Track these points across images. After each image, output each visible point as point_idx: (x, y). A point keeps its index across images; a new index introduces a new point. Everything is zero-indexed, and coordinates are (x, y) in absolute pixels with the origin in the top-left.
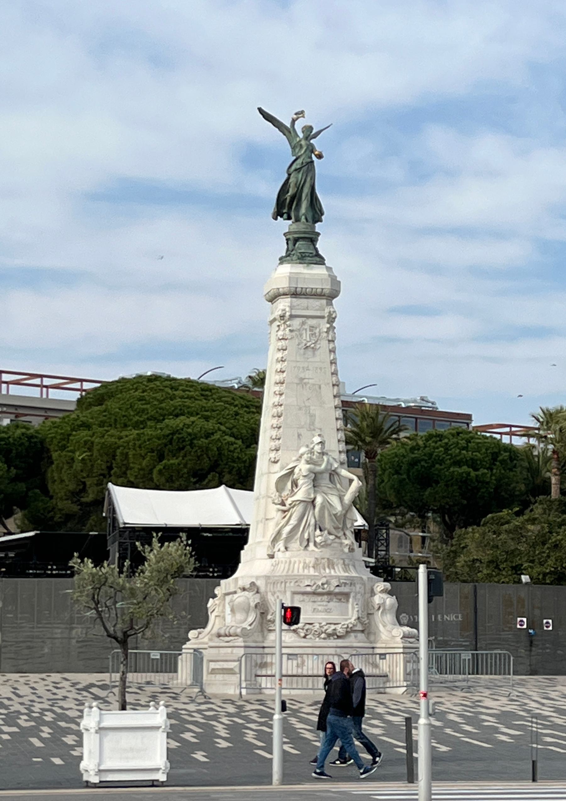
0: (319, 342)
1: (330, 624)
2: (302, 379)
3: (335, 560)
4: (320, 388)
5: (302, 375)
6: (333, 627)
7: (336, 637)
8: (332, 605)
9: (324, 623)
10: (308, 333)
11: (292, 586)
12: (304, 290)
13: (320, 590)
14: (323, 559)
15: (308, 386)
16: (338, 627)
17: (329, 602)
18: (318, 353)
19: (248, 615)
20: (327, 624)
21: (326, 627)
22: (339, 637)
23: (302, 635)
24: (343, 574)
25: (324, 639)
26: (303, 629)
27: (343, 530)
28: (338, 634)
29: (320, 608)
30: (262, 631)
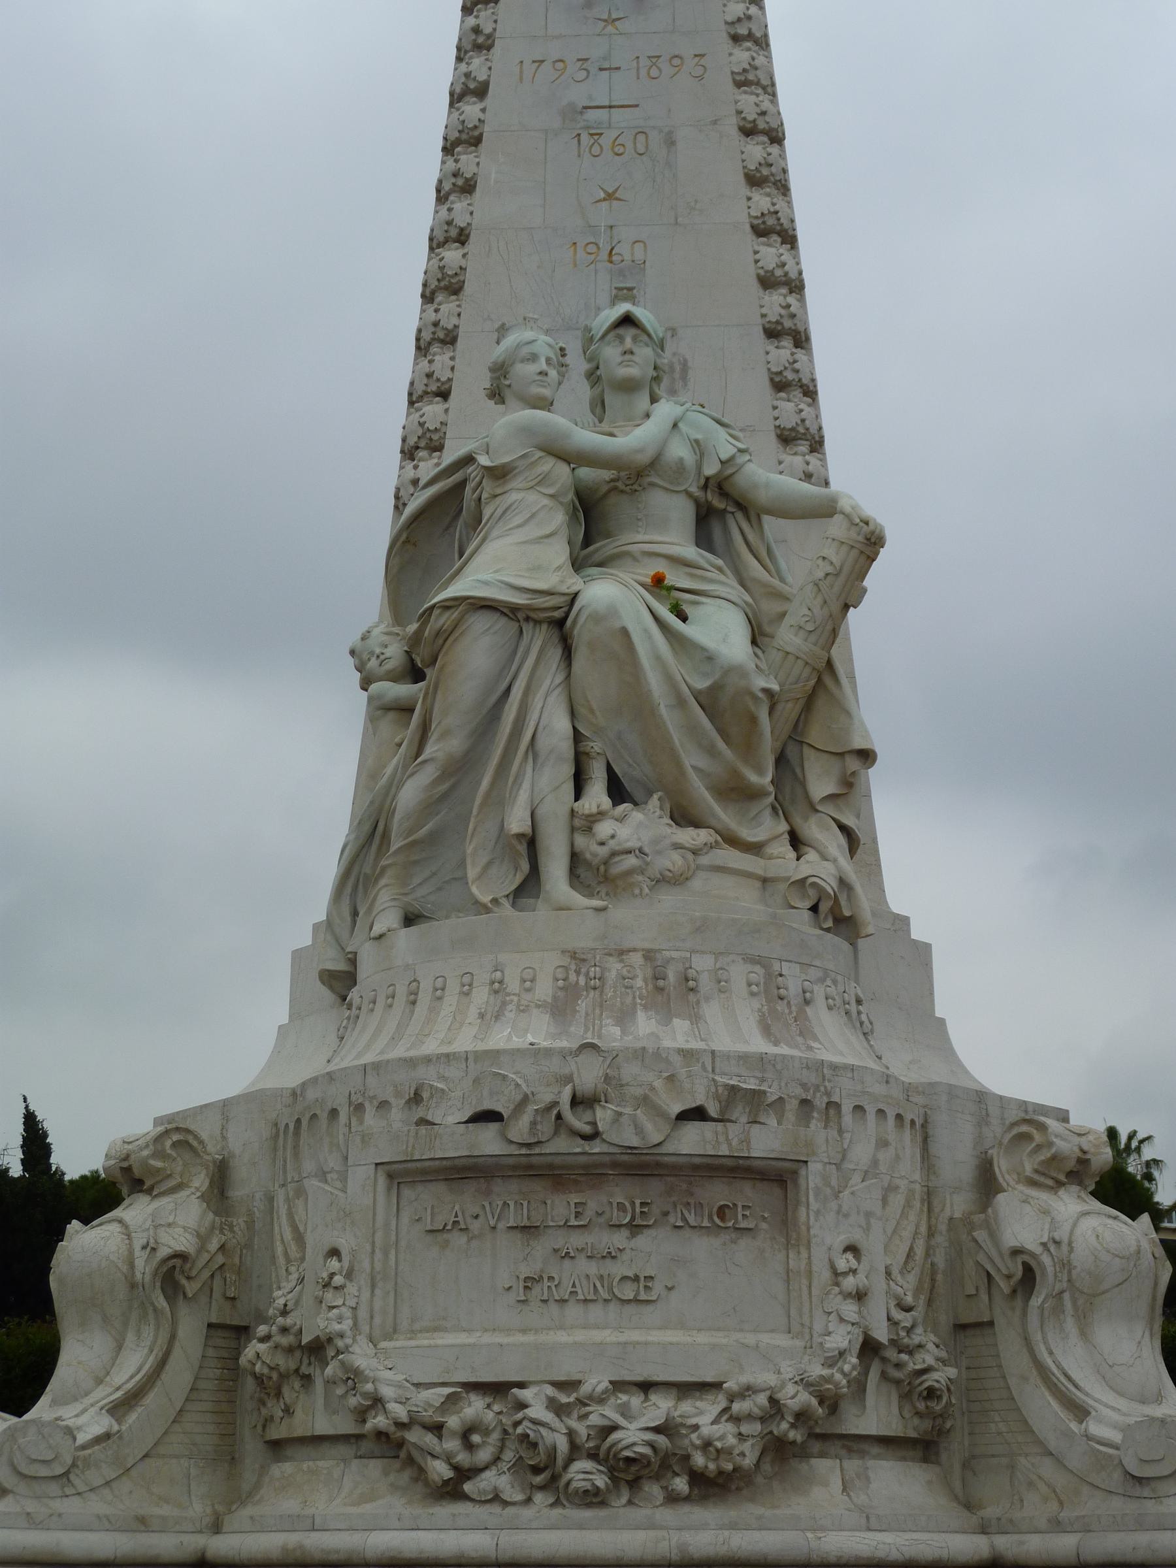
1: (646, 1387)
2: (574, 112)
3: (702, 963)
5: (577, 95)
6: (661, 1407)
7: (681, 1484)
8: (651, 1251)
9: (596, 1382)
11: (387, 1135)
13: (563, 1145)
14: (621, 953)
15: (606, 141)
16: (703, 1414)
17: (635, 1228)
19: (119, 1347)
20: (618, 1386)
21: (599, 1415)
22: (713, 1485)
23: (440, 1470)
24: (759, 1045)
25: (592, 1498)
26: (437, 1429)
27: (780, 809)
28: (699, 1460)
30: (226, 1456)
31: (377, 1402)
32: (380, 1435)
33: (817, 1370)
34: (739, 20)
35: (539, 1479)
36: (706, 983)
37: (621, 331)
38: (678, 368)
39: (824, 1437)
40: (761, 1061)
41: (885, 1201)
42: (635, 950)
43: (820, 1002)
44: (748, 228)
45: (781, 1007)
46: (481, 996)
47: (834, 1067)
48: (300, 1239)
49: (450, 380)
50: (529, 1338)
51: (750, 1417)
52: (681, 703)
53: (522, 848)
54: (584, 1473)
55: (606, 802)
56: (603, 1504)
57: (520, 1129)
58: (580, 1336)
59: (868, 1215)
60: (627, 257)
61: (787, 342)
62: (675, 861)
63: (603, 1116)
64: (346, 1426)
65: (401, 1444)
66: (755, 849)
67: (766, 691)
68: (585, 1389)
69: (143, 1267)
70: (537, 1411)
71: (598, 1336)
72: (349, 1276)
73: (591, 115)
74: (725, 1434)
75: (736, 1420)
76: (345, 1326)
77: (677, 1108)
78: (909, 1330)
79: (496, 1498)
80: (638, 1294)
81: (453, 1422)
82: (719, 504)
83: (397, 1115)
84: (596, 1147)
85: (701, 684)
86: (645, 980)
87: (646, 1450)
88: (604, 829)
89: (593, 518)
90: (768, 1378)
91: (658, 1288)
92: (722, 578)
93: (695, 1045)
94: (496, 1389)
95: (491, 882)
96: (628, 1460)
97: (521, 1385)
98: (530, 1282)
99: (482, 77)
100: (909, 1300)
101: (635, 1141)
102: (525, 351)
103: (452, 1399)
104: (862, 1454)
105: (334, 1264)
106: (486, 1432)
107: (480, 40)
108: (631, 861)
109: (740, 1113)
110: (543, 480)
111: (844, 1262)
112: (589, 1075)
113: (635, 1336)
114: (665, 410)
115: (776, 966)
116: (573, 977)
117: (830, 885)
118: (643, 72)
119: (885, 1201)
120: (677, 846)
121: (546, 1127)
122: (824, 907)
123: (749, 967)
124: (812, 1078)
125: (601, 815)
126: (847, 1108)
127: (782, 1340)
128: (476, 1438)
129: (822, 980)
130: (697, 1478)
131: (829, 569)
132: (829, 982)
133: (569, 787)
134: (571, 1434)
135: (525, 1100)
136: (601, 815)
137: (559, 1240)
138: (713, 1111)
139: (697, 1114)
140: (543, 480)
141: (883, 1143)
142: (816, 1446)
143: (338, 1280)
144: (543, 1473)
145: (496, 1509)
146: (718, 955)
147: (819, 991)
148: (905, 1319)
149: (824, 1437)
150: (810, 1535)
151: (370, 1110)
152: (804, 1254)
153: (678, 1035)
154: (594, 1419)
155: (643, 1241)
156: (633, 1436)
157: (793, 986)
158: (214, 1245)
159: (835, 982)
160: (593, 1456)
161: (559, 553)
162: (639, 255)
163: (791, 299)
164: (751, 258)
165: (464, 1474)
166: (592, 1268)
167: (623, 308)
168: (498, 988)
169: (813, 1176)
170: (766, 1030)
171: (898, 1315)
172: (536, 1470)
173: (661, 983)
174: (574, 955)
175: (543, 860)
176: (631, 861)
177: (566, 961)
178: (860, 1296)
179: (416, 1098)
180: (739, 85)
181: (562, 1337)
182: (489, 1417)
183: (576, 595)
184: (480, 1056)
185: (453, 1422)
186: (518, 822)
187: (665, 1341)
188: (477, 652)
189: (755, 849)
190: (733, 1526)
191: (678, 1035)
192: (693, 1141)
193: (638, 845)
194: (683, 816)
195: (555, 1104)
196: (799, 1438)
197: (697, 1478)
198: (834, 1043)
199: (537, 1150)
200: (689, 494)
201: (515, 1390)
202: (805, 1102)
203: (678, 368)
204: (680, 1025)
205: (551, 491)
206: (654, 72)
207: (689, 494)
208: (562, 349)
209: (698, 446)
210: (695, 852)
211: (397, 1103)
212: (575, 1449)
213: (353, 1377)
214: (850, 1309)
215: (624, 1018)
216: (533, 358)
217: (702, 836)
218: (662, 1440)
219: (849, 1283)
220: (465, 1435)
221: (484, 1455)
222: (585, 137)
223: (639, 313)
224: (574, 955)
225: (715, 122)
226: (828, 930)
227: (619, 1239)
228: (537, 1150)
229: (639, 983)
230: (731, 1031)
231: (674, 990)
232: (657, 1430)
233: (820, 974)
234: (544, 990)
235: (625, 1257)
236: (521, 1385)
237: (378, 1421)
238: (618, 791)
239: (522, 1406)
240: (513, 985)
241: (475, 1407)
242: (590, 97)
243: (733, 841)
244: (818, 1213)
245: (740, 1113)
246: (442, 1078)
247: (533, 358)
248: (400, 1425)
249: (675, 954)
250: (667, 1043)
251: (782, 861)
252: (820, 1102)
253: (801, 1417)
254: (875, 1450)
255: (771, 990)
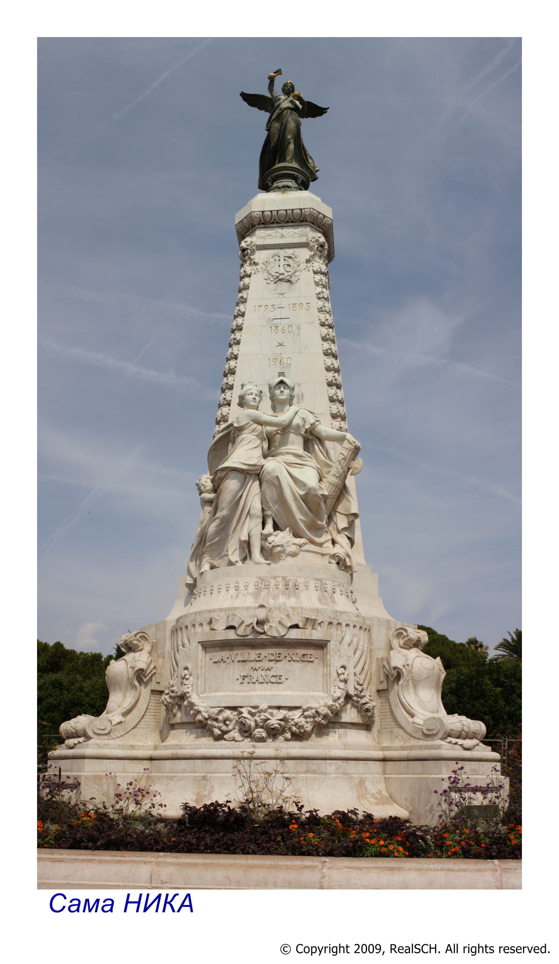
0: (298, 273)
1: (279, 708)
3: (301, 581)
4: (299, 329)
6: (282, 713)
7: (288, 735)
8: (280, 668)
10: (282, 263)
12: (275, 213)
14: (275, 577)
15: (280, 328)
16: (296, 715)
18: (297, 286)
20: (270, 707)
22: (299, 736)
24: (318, 605)
25: (262, 740)
26: (216, 720)
28: (294, 729)
29: (255, 675)
31: (199, 712)
32: (200, 721)
33: (330, 702)
34: (320, 293)
35: (246, 735)
36: (302, 587)
37: (280, 385)
38: (300, 395)
39: (334, 723)
40: (317, 611)
41: (355, 653)
42: (279, 577)
43: (338, 592)
44: (322, 354)
45: (325, 594)
46: (232, 591)
47: (340, 612)
48: (177, 665)
49: (231, 400)
50: (244, 694)
51: (309, 717)
52: (295, 499)
53: (245, 545)
54: (260, 732)
55: (271, 530)
56: (265, 741)
57: (241, 631)
58: (259, 693)
59: (349, 657)
60: (286, 362)
61: (335, 388)
62: (293, 549)
63: (266, 627)
64: (190, 719)
65: (206, 724)
66: (320, 545)
67: (322, 495)
68: (260, 708)
69: (131, 673)
70: (245, 714)
71: (264, 693)
72: (190, 675)
73: (275, 321)
74: (302, 721)
75: (306, 717)
76: (189, 690)
77: (289, 625)
78: (361, 691)
79: (234, 740)
80: (278, 680)
81: (220, 717)
82: (310, 437)
83: (206, 628)
84: (264, 637)
85: (302, 493)
86: (282, 586)
87: (278, 726)
88: (270, 539)
89: (272, 444)
90: (315, 705)
91: (283, 679)
92: (310, 460)
93: (296, 605)
94: (234, 708)
95: (235, 557)
96: (272, 728)
97: (241, 707)
98: (244, 677)
99: (243, 311)
100: (361, 682)
101: (276, 634)
102: (249, 392)
103: (220, 712)
104: (346, 728)
105: (186, 672)
106: (231, 721)
107: (243, 300)
108: (279, 549)
109: (309, 627)
110: (254, 431)
111: (341, 671)
112: (262, 614)
113: (276, 693)
114: (293, 409)
115: (324, 582)
116: (260, 585)
117: (343, 556)
118: (291, 308)
119: (355, 653)
120: (294, 544)
121: (249, 630)
122: (341, 563)
123: (316, 582)
124: (332, 615)
125: (270, 535)
126: (344, 624)
127: (321, 694)
128: (227, 722)
129: (339, 586)
130: (293, 734)
131: (343, 457)
132: (341, 586)
133: (260, 526)
134: (256, 721)
135: (243, 622)
136: (270, 535)
137: (254, 665)
138: (301, 625)
139: (296, 626)
140: (254, 431)
141: (354, 635)
142: (331, 725)
143: (187, 677)
144: (246, 732)
145: (233, 742)
146: (305, 578)
147: (338, 589)
148: (360, 688)
149: (334, 723)
150: (327, 750)
151: (197, 626)
152: (329, 668)
153: (292, 602)
154: (262, 717)
155: (279, 664)
156: (274, 722)
157: (329, 588)
158: (152, 667)
159: (343, 586)
160: (262, 727)
161: (258, 452)
162: (289, 362)
163: (336, 374)
164: (324, 362)
165: (225, 733)
166: (263, 673)
167: (281, 378)
168: (237, 588)
169: (331, 646)
170: (320, 600)
171: (358, 687)
172: (246, 732)
173: (287, 587)
174: (260, 578)
175: (252, 548)
176: (279, 549)
177: (258, 580)
178: (345, 681)
179: (210, 622)
180: (319, 312)
181: (253, 693)
182: (231, 716)
183: (263, 466)
184: (230, 609)
185: (220, 717)
186: (244, 537)
187: (285, 694)
188: (231, 485)
189: (320, 545)
190: (304, 748)
191: (292, 602)
192: (294, 634)
193: (281, 544)
194: (296, 535)
195: (252, 623)
196: (328, 723)
197: (293, 734)
198: (342, 603)
199: (246, 638)
200: (301, 435)
201: (239, 709)
202: (330, 623)
203: (300, 395)
204: (293, 599)
205: (256, 434)
206: (294, 308)
207: (301, 435)
208: (261, 391)
209: (304, 420)
210: (300, 546)
211: (205, 624)
212: (257, 726)
213: (192, 705)
214: (342, 685)
215: (275, 597)
216: (252, 394)
217: (303, 541)
218: (282, 723)
219: (342, 677)
220: (224, 722)
221: (231, 727)
222: (273, 327)
223: (285, 379)
224: (260, 578)
225: (312, 323)
226: (342, 570)
227: (272, 664)
228: (246, 638)
229: (281, 587)
230: (309, 601)
231: (291, 588)
232: (281, 720)
233: (339, 584)
234: (251, 589)
235: (273, 669)
236: (241, 707)
237: (199, 717)
238: (276, 527)
239: (241, 713)
240: (242, 587)
241: (228, 713)
242: (275, 316)
243: (312, 542)
244: (333, 656)
245: (309, 627)
246: (219, 616)
247: (252, 394)
248: (206, 719)
249: (292, 578)
250: (288, 605)
251: (329, 548)
252: (335, 622)
253: (325, 717)
254: (350, 726)
255: (322, 588)
